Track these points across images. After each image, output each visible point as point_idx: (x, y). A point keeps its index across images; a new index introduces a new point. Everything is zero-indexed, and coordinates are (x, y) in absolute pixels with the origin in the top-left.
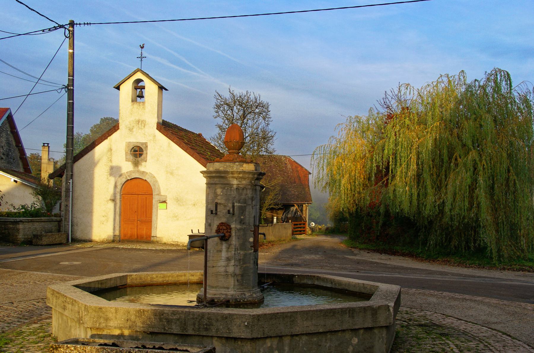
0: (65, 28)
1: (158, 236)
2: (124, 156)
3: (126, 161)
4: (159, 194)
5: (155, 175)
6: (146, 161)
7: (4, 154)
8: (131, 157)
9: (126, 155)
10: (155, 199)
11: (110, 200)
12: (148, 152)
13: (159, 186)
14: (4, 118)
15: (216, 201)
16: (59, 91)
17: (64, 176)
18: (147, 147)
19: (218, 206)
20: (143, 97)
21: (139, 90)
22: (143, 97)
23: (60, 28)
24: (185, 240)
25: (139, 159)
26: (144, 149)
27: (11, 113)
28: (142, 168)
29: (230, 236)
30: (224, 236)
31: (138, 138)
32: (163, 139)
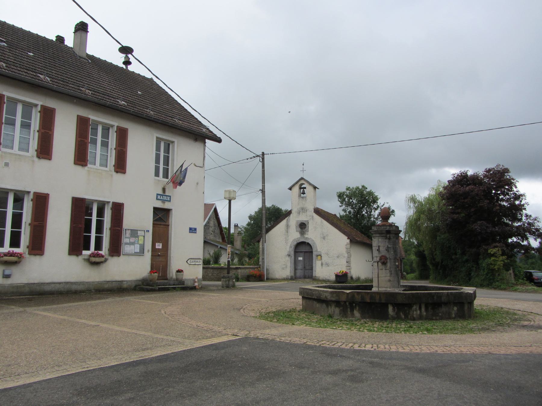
0: (260, 157)
1: (317, 276)
2: (295, 229)
3: (296, 231)
4: (316, 251)
5: (314, 240)
6: (308, 231)
7: (212, 231)
8: (299, 229)
9: (296, 228)
10: (315, 253)
11: (288, 255)
12: (309, 226)
13: (316, 246)
14: (213, 209)
15: (379, 245)
16: (257, 192)
17: (261, 241)
18: (308, 223)
19: (380, 247)
20: (305, 193)
21: (302, 190)
22: (305, 193)
23: (257, 156)
24: (333, 278)
25: (304, 230)
26: (307, 224)
27: (216, 206)
28: (306, 236)
29: (387, 262)
30: (384, 262)
31: (303, 218)
32: (317, 218)
